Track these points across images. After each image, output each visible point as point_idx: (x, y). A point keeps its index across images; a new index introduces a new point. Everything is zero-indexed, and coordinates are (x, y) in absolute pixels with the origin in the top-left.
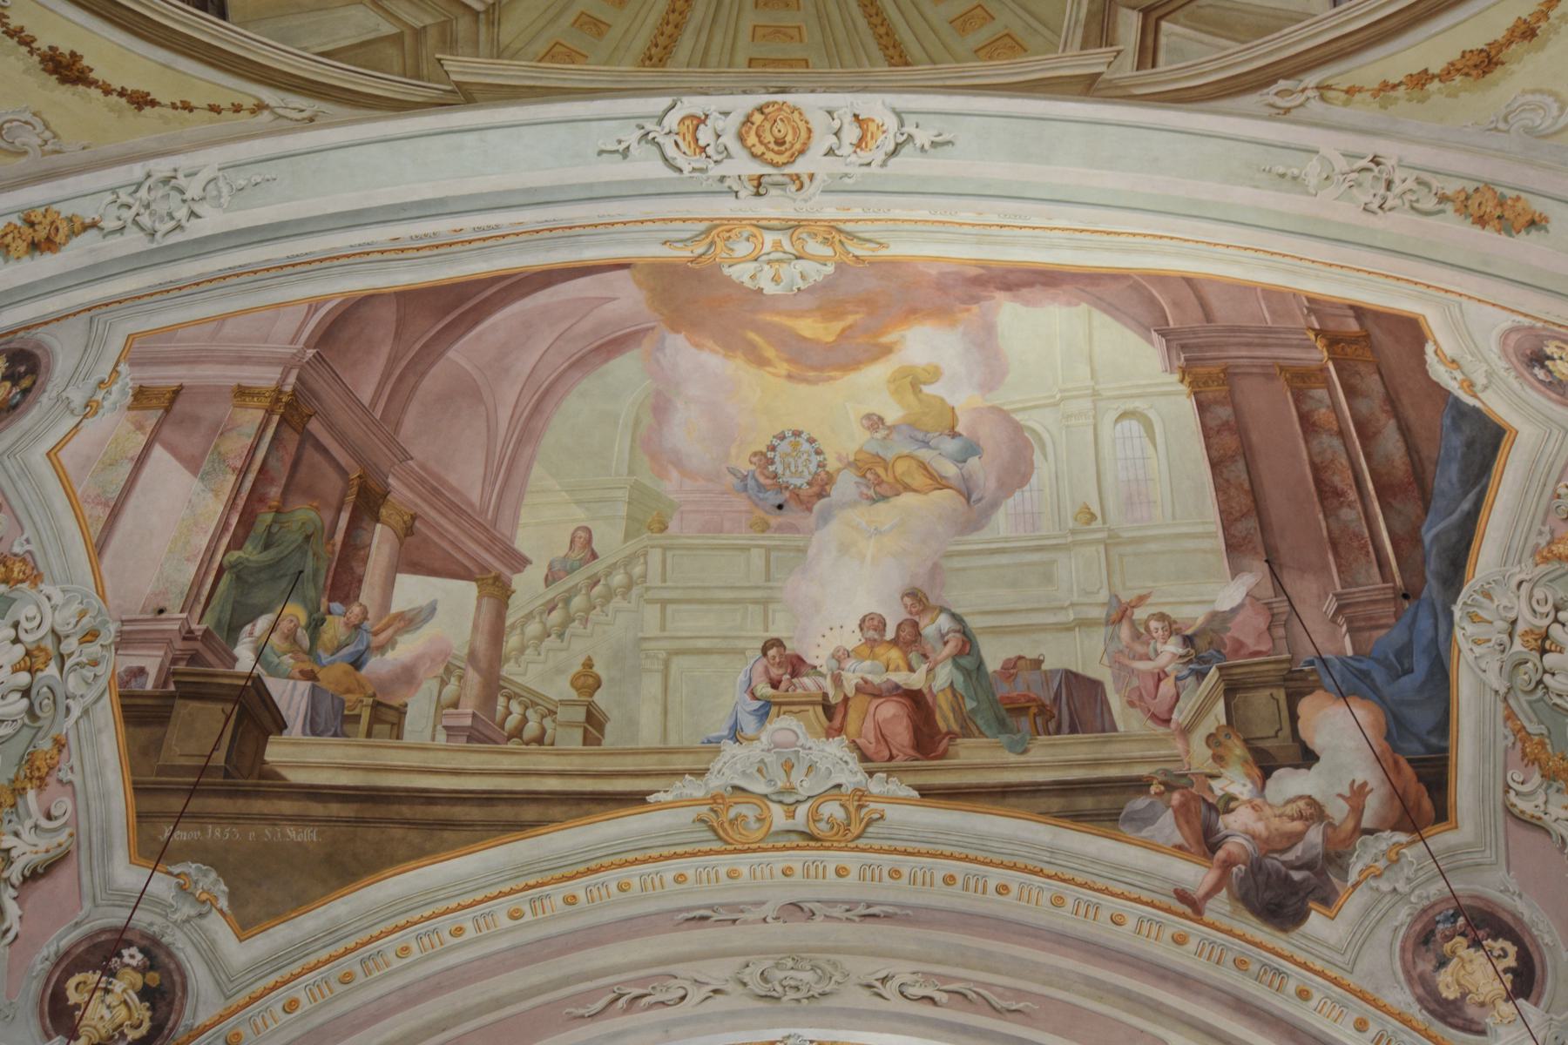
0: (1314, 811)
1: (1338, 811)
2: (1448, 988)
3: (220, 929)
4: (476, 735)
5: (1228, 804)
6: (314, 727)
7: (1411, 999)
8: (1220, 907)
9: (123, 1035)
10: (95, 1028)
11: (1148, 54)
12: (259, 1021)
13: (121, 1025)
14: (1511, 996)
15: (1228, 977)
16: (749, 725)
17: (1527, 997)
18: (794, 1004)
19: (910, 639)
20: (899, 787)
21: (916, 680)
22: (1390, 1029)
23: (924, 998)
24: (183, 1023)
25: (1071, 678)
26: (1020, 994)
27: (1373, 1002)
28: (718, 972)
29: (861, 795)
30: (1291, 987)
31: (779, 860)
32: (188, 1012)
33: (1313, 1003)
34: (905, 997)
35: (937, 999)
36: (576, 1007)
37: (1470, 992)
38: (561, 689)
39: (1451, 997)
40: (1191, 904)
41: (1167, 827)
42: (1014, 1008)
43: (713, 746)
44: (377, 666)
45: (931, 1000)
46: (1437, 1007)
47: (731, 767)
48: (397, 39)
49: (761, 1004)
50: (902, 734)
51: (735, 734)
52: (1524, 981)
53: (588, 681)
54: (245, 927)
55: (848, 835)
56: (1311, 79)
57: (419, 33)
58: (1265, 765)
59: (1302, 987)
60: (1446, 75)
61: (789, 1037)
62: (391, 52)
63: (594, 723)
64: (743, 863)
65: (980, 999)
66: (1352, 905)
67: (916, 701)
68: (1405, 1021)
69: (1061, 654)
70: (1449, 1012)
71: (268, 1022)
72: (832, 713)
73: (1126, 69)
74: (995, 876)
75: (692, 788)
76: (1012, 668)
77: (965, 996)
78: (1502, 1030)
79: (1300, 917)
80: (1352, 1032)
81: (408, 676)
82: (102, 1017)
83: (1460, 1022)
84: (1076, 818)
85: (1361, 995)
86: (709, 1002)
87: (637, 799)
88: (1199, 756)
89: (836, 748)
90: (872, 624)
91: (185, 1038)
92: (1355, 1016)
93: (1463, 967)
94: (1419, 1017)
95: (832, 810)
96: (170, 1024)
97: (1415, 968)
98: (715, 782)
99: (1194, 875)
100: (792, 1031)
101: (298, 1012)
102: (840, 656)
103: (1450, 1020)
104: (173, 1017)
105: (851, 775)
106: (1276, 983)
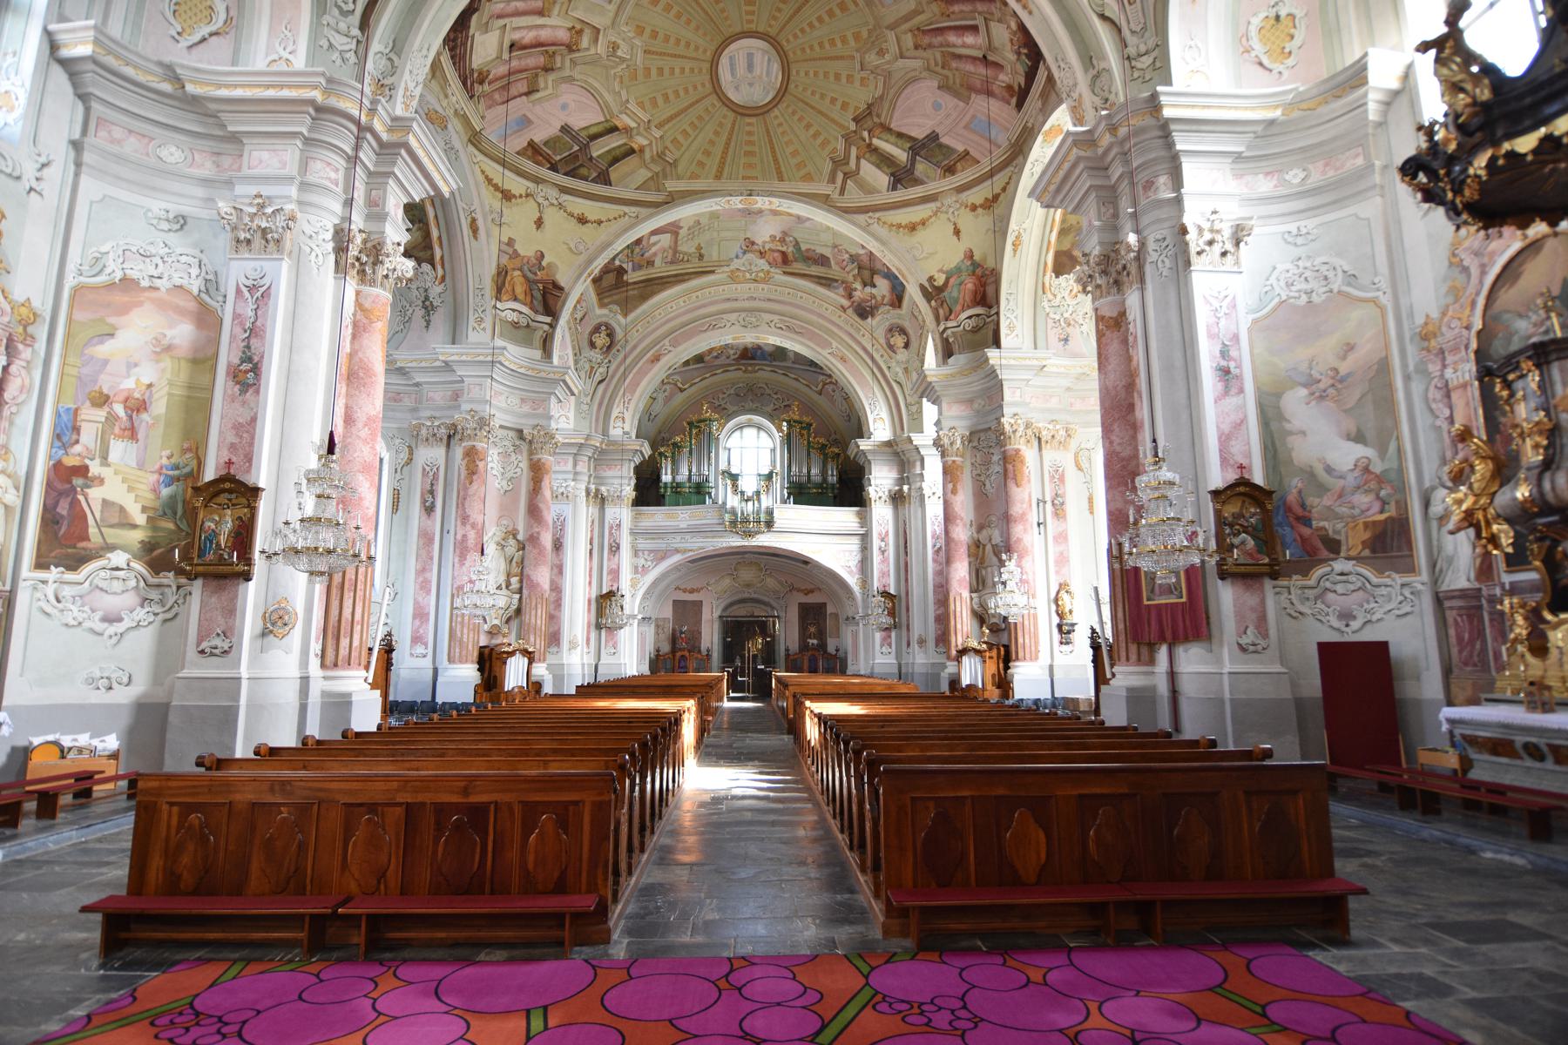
0: (873, 297)
1: (879, 298)
2: (892, 341)
3: (620, 317)
4: (672, 263)
5: (856, 290)
6: (634, 270)
8: (850, 311)
11: (842, 192)
15: (848, 328)
16: (740, 255)
19: (782, 241)
20: (777, 271)
21: (784, 249)
25: (822, 256)
26: (802, 327)
28: (733, 317)
29: (768, 272)
31: (748, 286)
38: (693, 250)
40: (844, 309)
41: (841, 291)
43: (731, 260)
44: (647, 255)
47: (736, 264)
48: (652, 178)
50: (779, 259)
51: (737, 257)
52: (907, 346)
53: (699, 248)
54: (625, 315)
55: (765, 281)
56: (877, 215)
57: (657, 174)
58: (865, 285)
60: (906, 226)
62: (652, 183)
63: (701, 257)
64: (739, 286)
66: (878, 318)
67: (784, 254)
69: (820, 250)
70: (891, 347)
72: (762, 254)
73: (836, 196)
74: (800, 294)
75: (726, 269)
76: (808, 250)
79: (866, 318)
81: (655, 254)
84: (821, 284)
87: (712, 272)
88: (850, 278)
89: (763, 261)
90: (773, 238)
95: (762, 275)
98: (732, 267)
99: (846, 303)
102: (765, 242)
105: (766, 267)
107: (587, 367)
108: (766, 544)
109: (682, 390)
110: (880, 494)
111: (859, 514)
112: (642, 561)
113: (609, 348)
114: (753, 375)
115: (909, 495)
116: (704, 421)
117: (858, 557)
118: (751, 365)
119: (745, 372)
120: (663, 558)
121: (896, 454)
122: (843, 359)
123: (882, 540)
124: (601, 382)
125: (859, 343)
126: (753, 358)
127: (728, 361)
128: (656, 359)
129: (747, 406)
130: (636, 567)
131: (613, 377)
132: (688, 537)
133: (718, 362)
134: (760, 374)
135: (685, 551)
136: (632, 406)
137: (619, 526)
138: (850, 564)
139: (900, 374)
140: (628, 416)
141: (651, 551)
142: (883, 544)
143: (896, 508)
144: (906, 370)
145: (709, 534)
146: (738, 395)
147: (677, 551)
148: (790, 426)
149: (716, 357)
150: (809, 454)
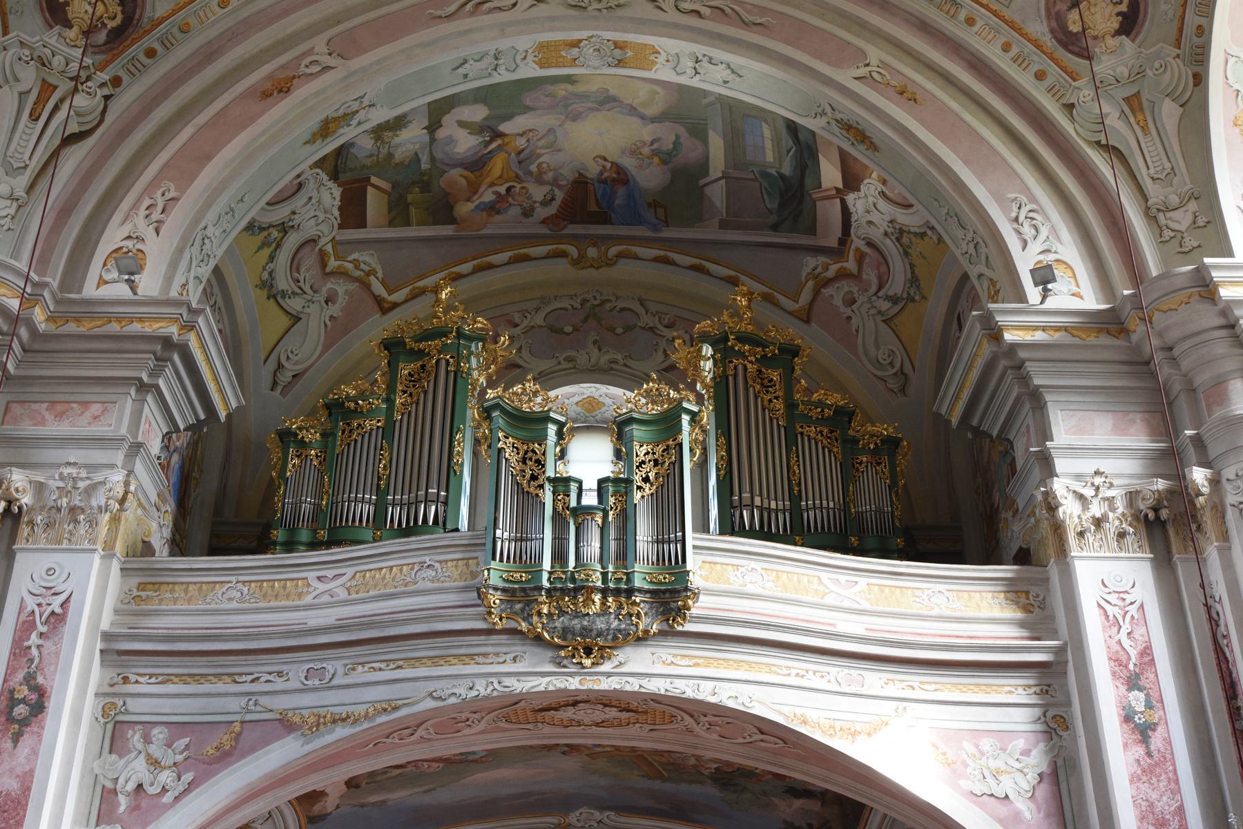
7: (1046, 29)
9: (104, 25)
10: (82, 19)
12: (202, 14)
13: (101, 17)
14: (1118, 33)
17: (1127, 36)
18: (596, 13)
22: (1026, 51)
23: (693, 11)
24: (146, 16)
27: (1019, 31)
30: (963, 15)
32: (148, 7)
33: (976, 28)
34: (679, 10)
35: (702, 13)
36: (436, 10)
37: (1089, 28)
39: (1075, 31)
42: (757, 22)
45: (698, 13)
46: (1063, 37)
49: (573, 12)
59: (970, 16)
61: (592, 37)
65: (734, 14)
68: (1038, 46)
71: (209, 15)
77: (723, 11)
78: (1104, 58)
80: (999, 51)
82: (86, 11)
83: (1077, 49)
85: (1011, 25)
86: (533, 9)
91: (149, 26)
92: (1004, 40)
93: (1089, 8)
94: (1049, 44)
96: (137, 16)
97: (1054, 7)
100: (594, 33)
101: (230, 8)
103: (1071, 48)
104: (138, 11)
106: (952, 12)
107: (29, 77)
108: (656, 686)
109: (385, 308)
110: (1096, 510)
111: (1016, 592)
112: (137, 770)
113: (120, 36)
114: (604, 273)
115: (1219, 510)
116: (441, 333)
117: (1037, 761)
118: (596, 241)
119: (576, 263)
120: (224, 757)
121: (1140, 365)
122: (906, 94)
123: (1133, 683)
124: (71, 140)
125: (956, 49)
126: (602, 218)
127: (530, 227)
128: (281, 87)
129: (582, 359)
130: (108, 795)
131: (123, 133)
132: (334, 665)
133: (497, 226)
134: (625, 269)
135: (321, 722)
136: (177, 220)
137: (57, 619)
138: (1007, 785)
139: (1114, 121)
140: (157, 250)
141: (178, 728)
142: (1137, 700)
143: (1164, 564)
144: (1134, 103)
145: (423, 649)
146: (554, 330)
147: (286, 725)
148: (724, 354)
149: (492, 209)
150: (791, 439)
